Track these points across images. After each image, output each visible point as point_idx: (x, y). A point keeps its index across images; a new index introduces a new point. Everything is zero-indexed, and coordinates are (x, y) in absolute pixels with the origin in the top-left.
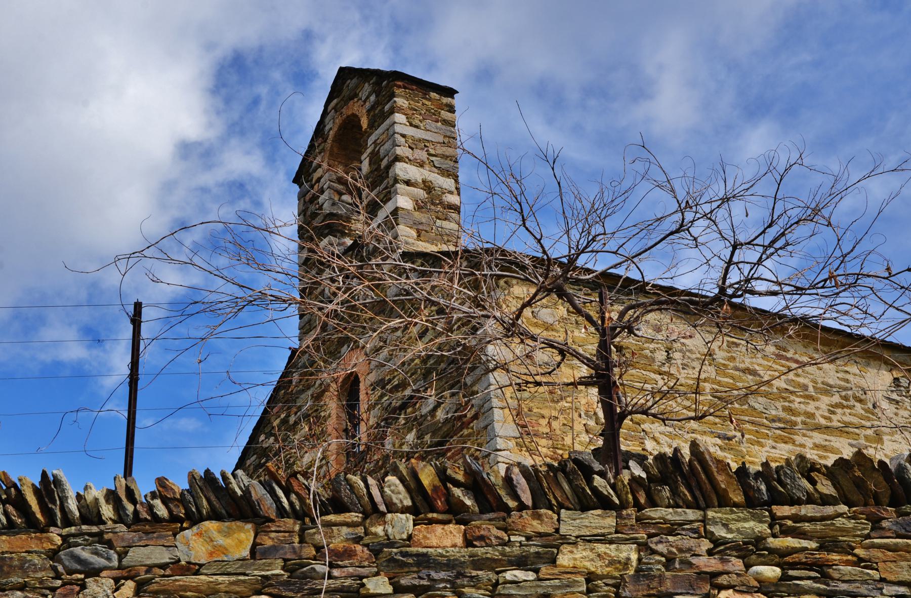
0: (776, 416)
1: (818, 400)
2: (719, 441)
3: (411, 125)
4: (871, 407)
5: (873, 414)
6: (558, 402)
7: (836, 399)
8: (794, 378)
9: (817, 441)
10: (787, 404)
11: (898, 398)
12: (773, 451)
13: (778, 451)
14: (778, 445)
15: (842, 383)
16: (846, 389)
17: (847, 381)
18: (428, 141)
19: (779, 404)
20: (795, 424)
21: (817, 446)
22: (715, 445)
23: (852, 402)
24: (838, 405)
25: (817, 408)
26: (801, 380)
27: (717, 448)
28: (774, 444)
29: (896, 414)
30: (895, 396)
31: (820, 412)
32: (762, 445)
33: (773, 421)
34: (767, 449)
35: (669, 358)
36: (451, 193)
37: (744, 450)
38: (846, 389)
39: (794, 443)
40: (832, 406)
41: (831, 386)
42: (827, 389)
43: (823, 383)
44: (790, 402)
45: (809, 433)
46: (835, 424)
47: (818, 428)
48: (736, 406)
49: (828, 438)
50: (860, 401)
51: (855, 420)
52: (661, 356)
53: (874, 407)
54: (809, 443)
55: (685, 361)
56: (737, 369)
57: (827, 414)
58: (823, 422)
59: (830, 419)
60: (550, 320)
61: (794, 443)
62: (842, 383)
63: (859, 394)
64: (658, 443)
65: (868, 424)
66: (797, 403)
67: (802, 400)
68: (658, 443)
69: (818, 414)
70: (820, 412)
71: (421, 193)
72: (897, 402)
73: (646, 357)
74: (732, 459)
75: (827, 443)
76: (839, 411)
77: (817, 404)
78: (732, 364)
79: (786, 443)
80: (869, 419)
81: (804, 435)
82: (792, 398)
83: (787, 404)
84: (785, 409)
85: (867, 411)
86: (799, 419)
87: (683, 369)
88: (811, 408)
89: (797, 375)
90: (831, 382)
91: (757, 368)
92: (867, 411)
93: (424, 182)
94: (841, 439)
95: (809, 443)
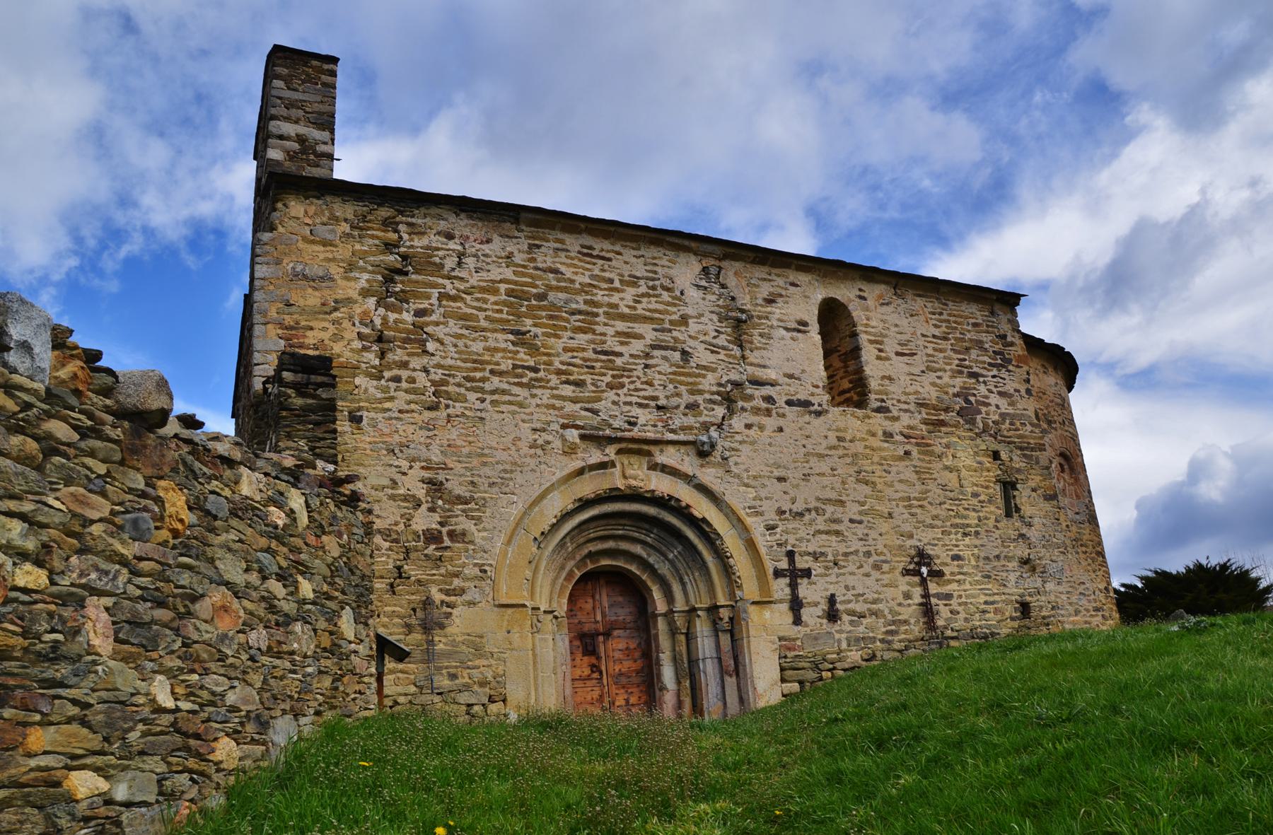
0: (575, 309)
1: (623, 291)
2: (511, 337)
3: (289, 88)
4: (679, 294)
5: (680, 300)
6: (330, 313)
7: (643, 289)
8: (599, 273)
9: (619, 329)
10: (589, 297)
11: (707, 285)
12: (572, 341)
13: (576, 342)
14: (577, 336)
15: (650, 275)
16: (653, 279)
17: (655, 272)
18: (305, 101)
19: (580, 299)
20: (597, 315)
21: (618, 334)
22: (506, 341)
23: (659, 291)
24: (643, 295)
25: (622, 299)
26: (607, 275)
27: (509, 343)
28: (572, 335)
29: (704, 299)
30: (703, 283)
31: (625, 302)
32: (558, 337)
33: (573, 314)
34: (565, 340)
35: (460, 264)
36: (325, 143)
37: (539, 343)
38: (653, 279)
39: (594, 332)
40: (638, 296)
41: (638, 278)
42: (633, 281)
43: (630, 276)
44: (592, 295)
45: (612, 322)
46: (640, 311)
47: (623, 317)
48: (534, 302)
49: (631, 325)
50: (668, 289)
51: (661, 307)
52: (450, 263)
53: (682, 293)
54: (610, 331)
55: (479, 265)
56: (537, 268)
57: (632, 304)
58: (627, 311)
59: (635, 308)
60: (329, 237)
61: (594, 332)
62: (650, 275)
63: (667, 283)
64: (442, 344)
65: (675, 309)
66: (599, 296)
67: (606, 293)
68: (442, 344)
69: (621, 304)
70: (625, 302)
71: (296, 146)
72: (706, 288)
73: (435, 264)
74: (525, 353)
75: (630, 330)
76: (645, 300)
77: (622, 295)
78: (532, 265)
79: (585, 333)
80: (675, 305)
81: (606, 325)
82: (595, 291)
83: (589, 297)
84: (586, 302)
85: (674, 298)
86: (601, 311)
87: (476, 272)
88: (615, 299)
89: (603, 270)
90: (638, 274)
91: (559, 266)
92: (674, 298)
93: (297, 135)
94: (645, 325)
95: (610, 331)
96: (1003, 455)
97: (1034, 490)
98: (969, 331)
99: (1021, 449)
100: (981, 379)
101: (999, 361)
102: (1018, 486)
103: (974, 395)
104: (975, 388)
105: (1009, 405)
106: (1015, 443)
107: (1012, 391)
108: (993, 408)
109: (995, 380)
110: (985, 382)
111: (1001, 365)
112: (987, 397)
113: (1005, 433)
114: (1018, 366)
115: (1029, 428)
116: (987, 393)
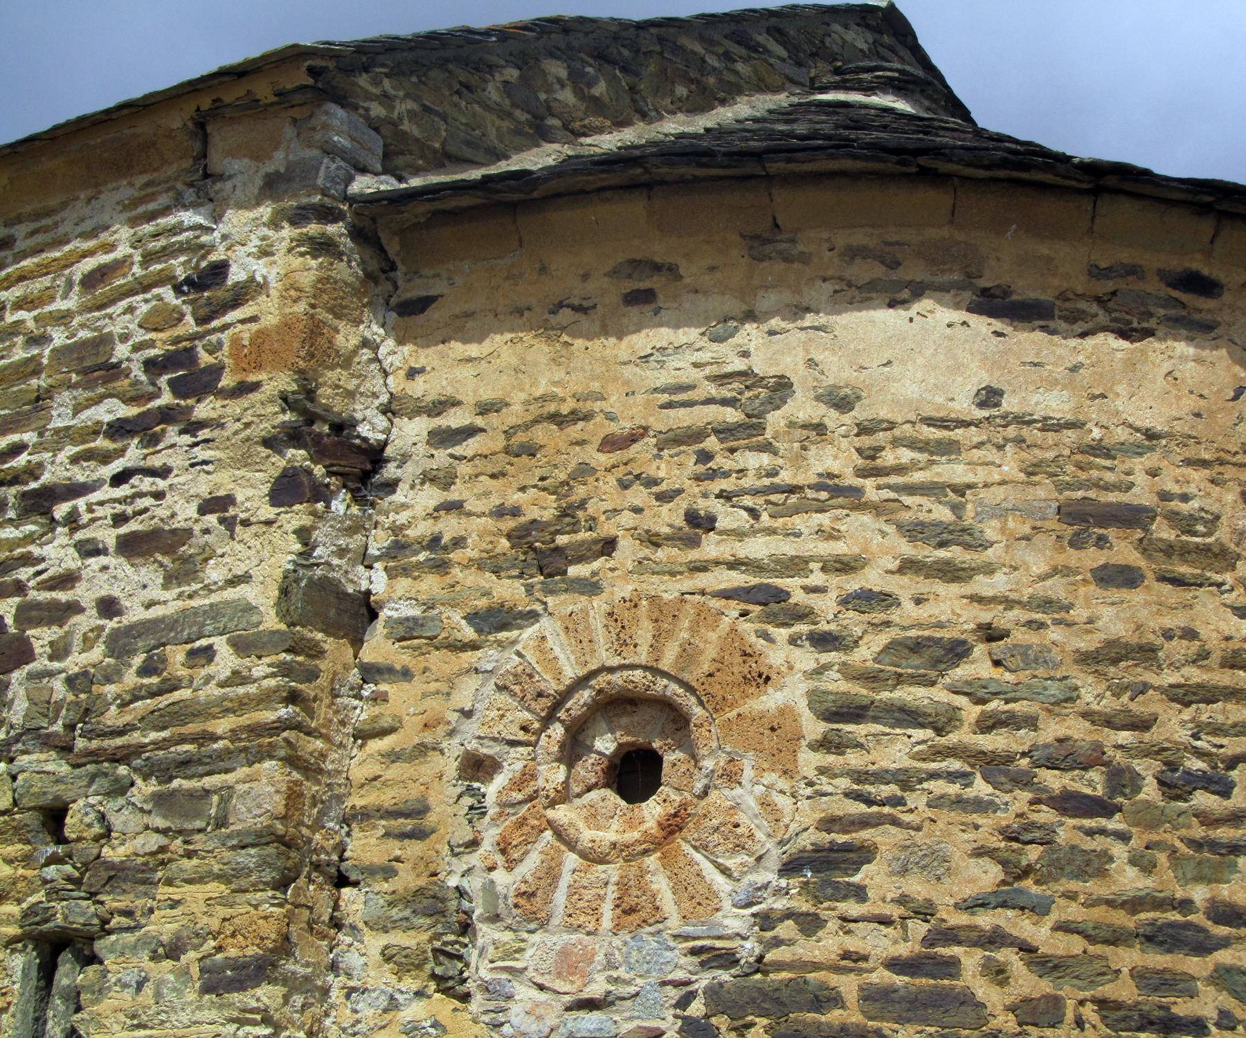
96: (72, 824)
97: (173, 951)
98: (63, 318)
99: (164, 772)
100: (61, 510)
101: (166, 398)
102: (100, 946)
103: (19, 588)
104: (28, 560)
105: (170, 580)
106: (140, 749)
107: (186, 512)
108: (85, 622)
109: (124, 490)
110: (72, 521)
111: (167, 415)
112: (68, 580)
113: (112, 717)
114: (244, 389)
115: (226, 660)
116: (72, 561)
